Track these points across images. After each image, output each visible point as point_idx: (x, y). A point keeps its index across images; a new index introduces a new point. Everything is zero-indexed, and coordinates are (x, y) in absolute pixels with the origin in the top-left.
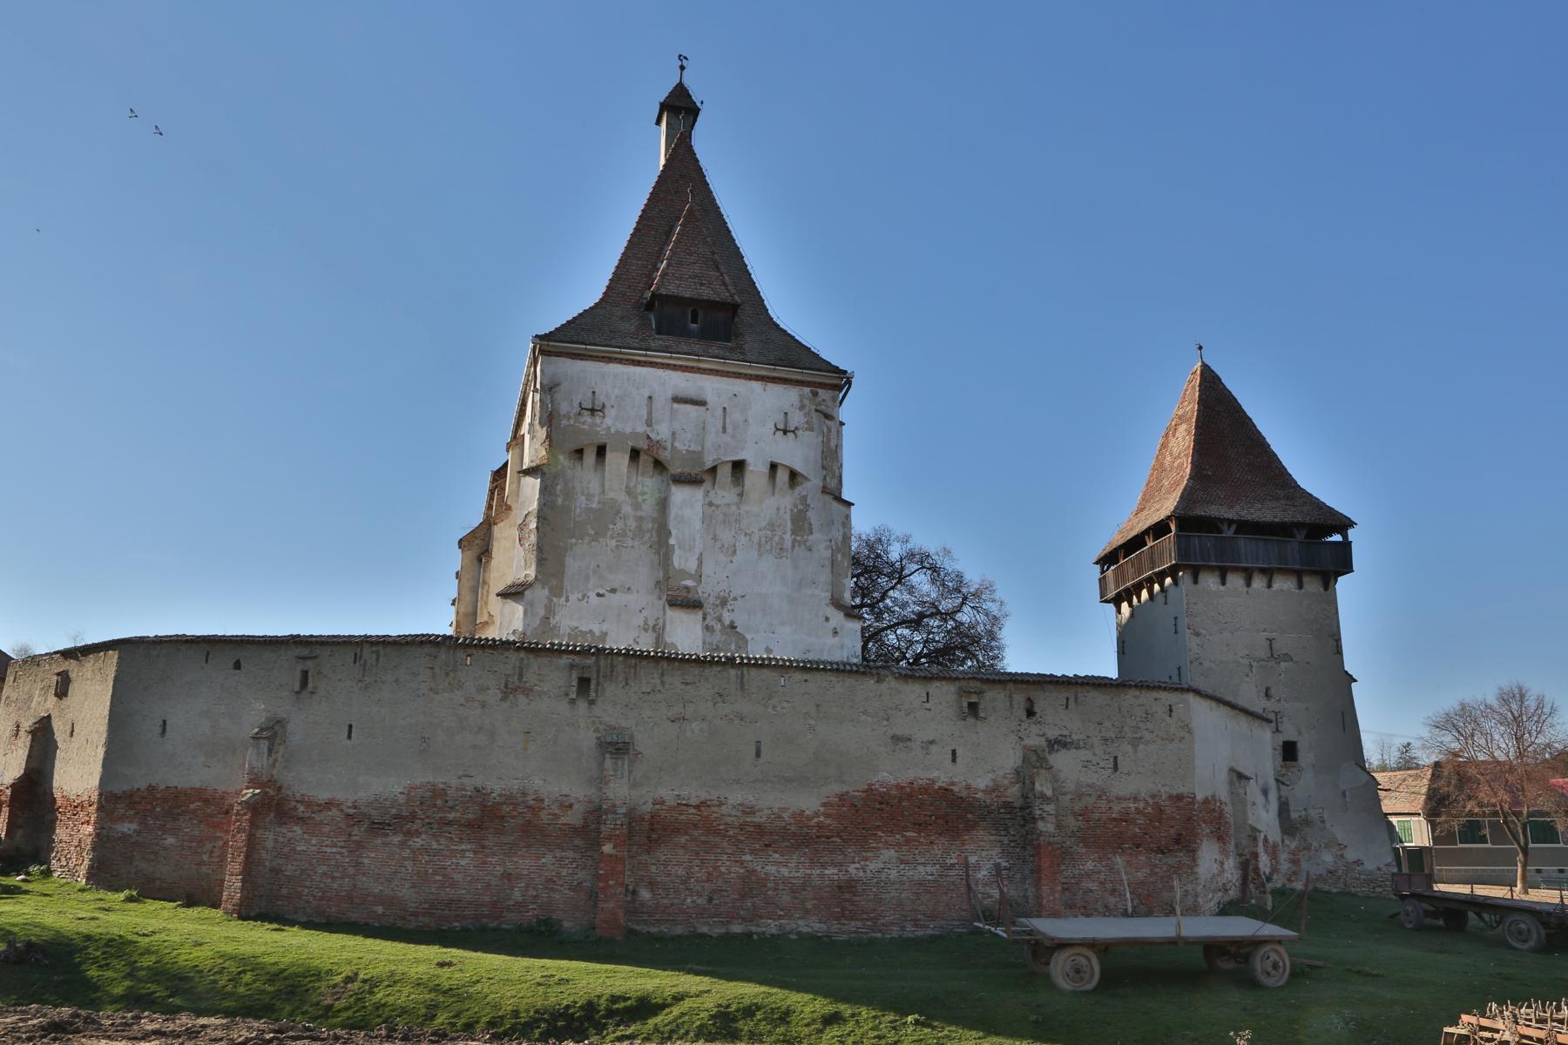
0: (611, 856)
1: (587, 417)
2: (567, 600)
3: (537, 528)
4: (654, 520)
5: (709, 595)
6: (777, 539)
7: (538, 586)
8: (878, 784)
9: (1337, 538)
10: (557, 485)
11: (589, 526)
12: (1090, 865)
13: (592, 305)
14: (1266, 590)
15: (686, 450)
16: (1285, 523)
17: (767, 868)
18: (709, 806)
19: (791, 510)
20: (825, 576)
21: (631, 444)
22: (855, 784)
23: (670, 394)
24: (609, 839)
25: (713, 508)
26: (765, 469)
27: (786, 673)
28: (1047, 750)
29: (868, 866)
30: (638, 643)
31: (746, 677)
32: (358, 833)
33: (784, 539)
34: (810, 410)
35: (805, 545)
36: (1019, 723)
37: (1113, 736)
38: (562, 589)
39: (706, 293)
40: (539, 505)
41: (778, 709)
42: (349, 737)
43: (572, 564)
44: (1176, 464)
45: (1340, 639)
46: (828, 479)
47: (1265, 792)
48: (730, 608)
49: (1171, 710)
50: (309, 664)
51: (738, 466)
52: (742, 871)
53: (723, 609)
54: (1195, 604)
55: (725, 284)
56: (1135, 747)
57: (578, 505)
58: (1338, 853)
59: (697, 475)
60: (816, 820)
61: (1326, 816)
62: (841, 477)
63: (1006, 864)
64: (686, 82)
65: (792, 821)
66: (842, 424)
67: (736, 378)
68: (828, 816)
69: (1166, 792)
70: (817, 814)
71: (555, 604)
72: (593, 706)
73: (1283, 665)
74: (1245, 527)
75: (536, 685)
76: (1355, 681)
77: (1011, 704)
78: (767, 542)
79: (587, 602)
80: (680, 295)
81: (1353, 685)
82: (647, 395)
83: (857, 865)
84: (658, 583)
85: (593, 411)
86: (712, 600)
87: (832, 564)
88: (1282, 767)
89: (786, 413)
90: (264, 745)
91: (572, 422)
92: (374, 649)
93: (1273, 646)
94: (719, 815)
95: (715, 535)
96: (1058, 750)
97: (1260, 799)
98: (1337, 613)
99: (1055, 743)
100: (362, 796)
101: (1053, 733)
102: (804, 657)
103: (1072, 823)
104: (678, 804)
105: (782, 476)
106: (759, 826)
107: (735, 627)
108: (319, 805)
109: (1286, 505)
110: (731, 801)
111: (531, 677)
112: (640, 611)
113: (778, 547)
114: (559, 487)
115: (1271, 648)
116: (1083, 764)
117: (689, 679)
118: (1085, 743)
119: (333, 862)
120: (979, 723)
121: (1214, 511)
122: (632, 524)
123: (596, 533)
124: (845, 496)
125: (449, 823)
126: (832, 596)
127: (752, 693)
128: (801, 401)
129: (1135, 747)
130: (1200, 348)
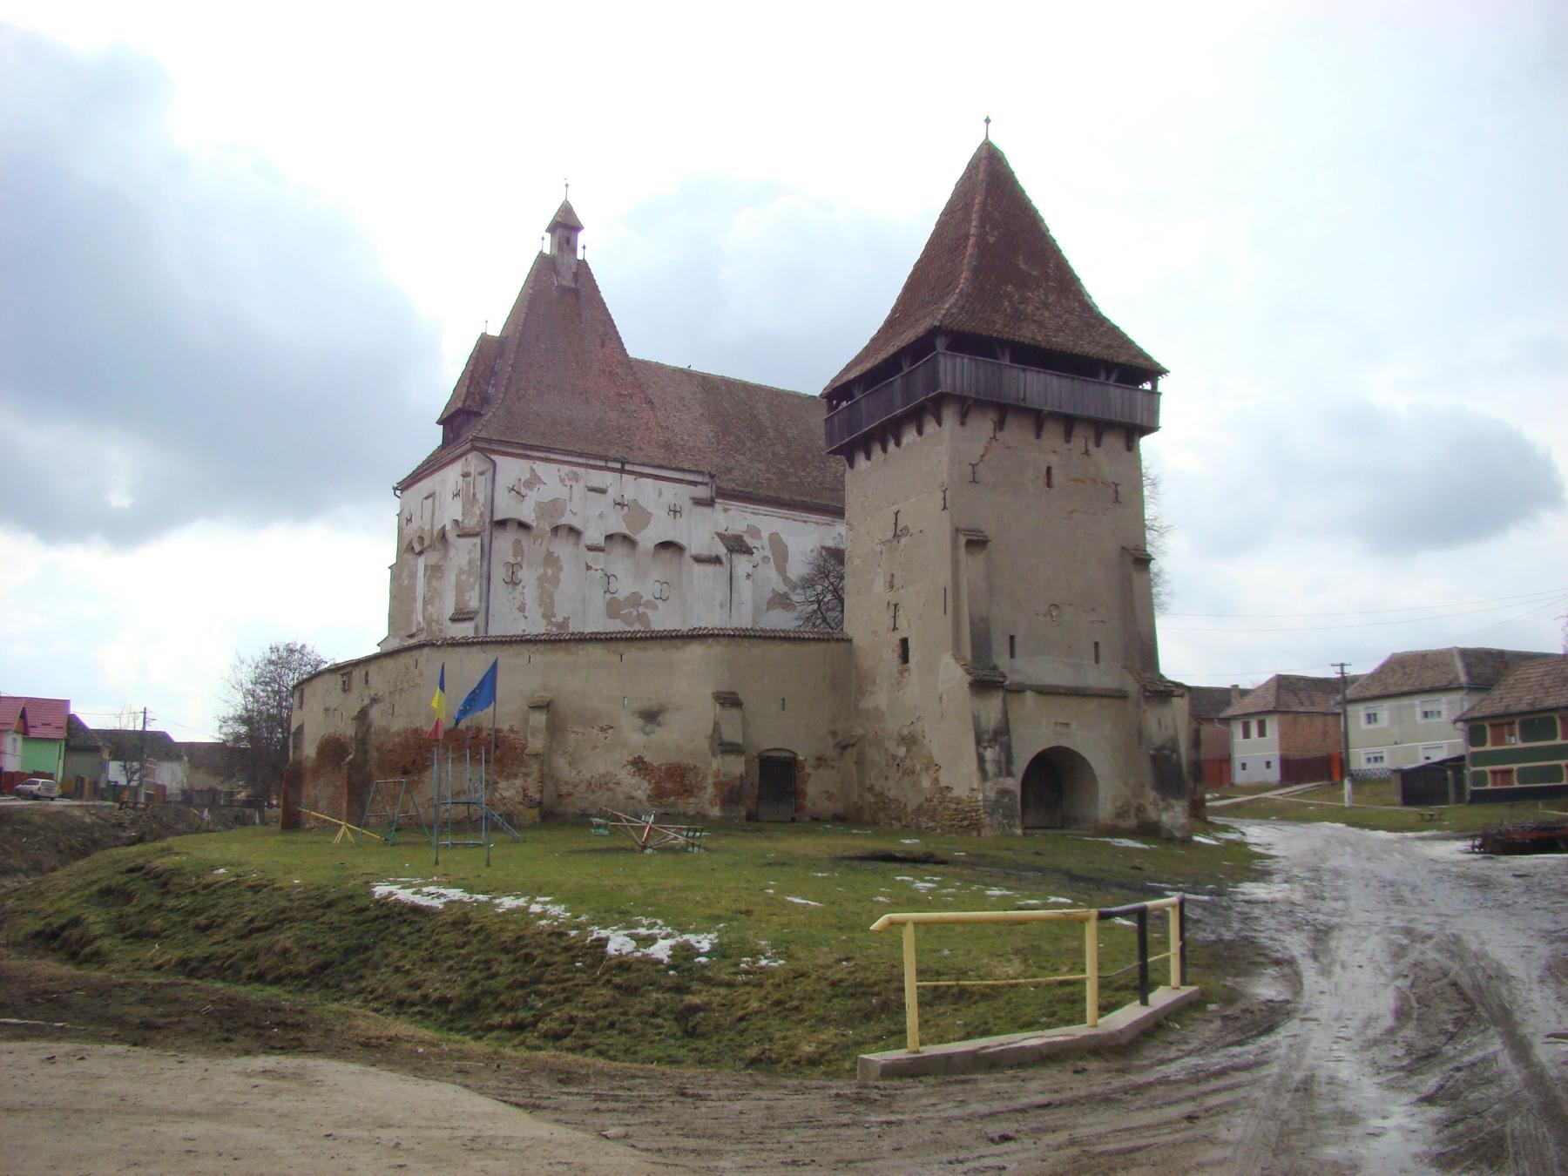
56: (400, 695)
129: (400, 695)
130: (988, 121)
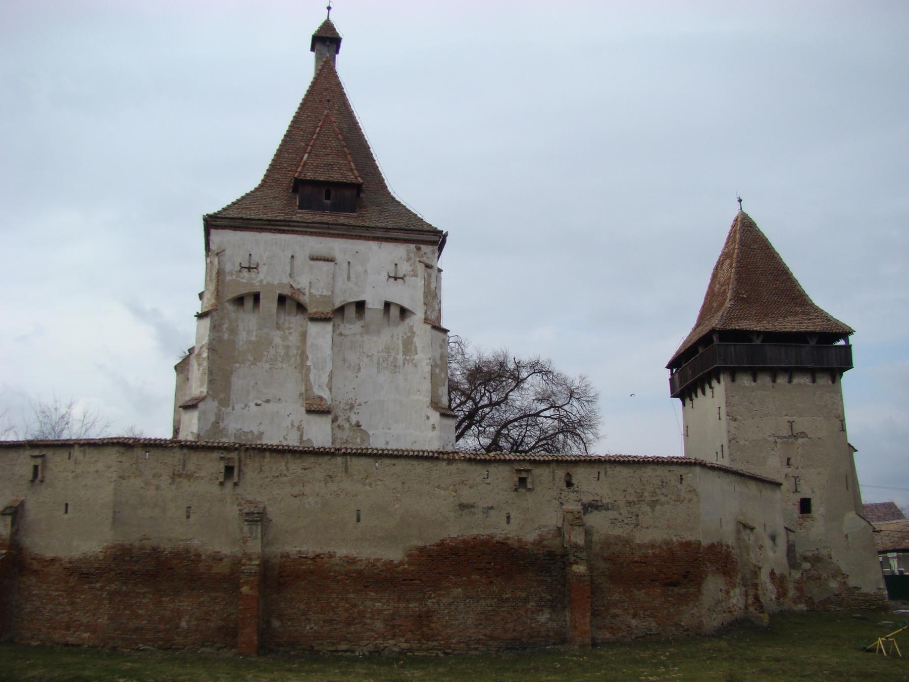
0: (248, 595)
1: (245, 273)
2: (233, 409)
3: (208, 357)
4: (298, 348)
5: (340, 402)
6: (391, 359)
7: (209, 400)
8: (449, 540)
9: (842, 343)
10: (223, 324)
11: (249, 354)
12: (616, 597)
13: (253, 189)
14: (788, 384)
15: (320, 295)
16: (801, 332)
17: (365, 603)
18: (322, 558)
19: (402, 336)
20: (426, 386)
21: (278, 292)
22: (431, 538)
23: (307, 253)
24: (246, 583)
25: (343, 337)
26: (381, 306)
27: (379, 459)
28: (582, 512)
29: (441, 600)
30: (286, 440)
31: (349, 463)
32: (72, 581)
33: (397, 359)
34: (415, 261)
35: (412, 363)
36: (560, 492)
37: (636, 499)
38: (230, 400)
39: (336, 177)
40: (209, 340)
41: (374, 486)
42: (66, 512)
43: (237, 382)
44: (721, 291)
45: (844, 420)
46: (429, 313)
47: (773, 538)
48: (357, 411)
49: (682, 479)
50: (39, 461)
51: (360, 306)
52: (347, 605)
53: (350, 412)
54: (733, 396)
55: (352, 170)
57: (241, 339)
58: (842, 581)
59: (328, 313)
60: (401, 567)
61: (833, 553)
62: (440, 310)
63: (550, 597)
64: (333, 19)
65: (384, 568)
66: (440, 271)
67: (358, 239)
68: (410, 564)
69: (677, 540)
70: (402, 563)
71: (223, 413)
72: (236, 487)
73: (800, 441)
74: (771, 337)
75: (195, 472)
76: (856, 451)
77: (554, 479)
78: (383, 361)
79: (248, 410)
80: (317, 179)
81: (855, 454)
82: (290, 256)
83: (434, 600)
84: (301, 394)
85: (249, 269)
86: (342, 406)
87: (431, 377)
88: (799, 518)
89: (396, 265)
90: (9, 519)
91: (234, 277)
92: (82, 449)
93: (793, 427)
94: (329, 565)
95: (344, 358)
96: (591, 512)
97: (768, 543)
98: (842, 400)
99: (589, 506)
100: (76, 554)
101: (586, 499)
102: (384, 447)
103: (602, 565)
104: (300, 557)
105: (395, 312)
106: (360, 573)
107: (360, 426)
108: (47, 561)
109: (803, 318)
110: (338, 555)
111: (191, 467)
112: (288, 416)
113: (393, 365)
114: (225, 326)
115: (792, 428)
116: (611, 521)
117: (306, 465)
118: (613, 506)
119: (56, 602)
120: (528, 493)
121: (745, 325)
122: (282, 352)
123: (255, 359)
124: (444, 325)
125: (134, 573)
126: (431, 400)
127: (354, 475)
128: (408, 255)
130: (740, 201)
